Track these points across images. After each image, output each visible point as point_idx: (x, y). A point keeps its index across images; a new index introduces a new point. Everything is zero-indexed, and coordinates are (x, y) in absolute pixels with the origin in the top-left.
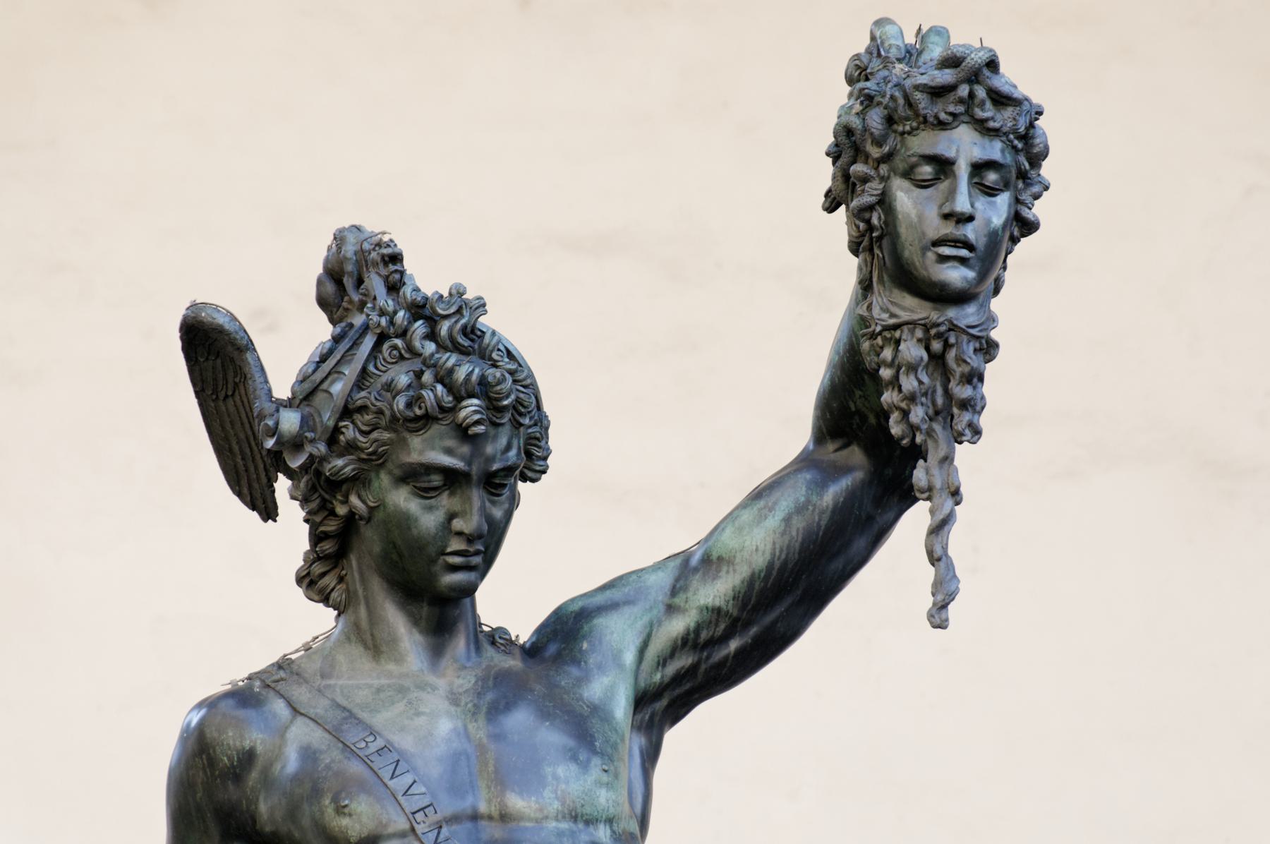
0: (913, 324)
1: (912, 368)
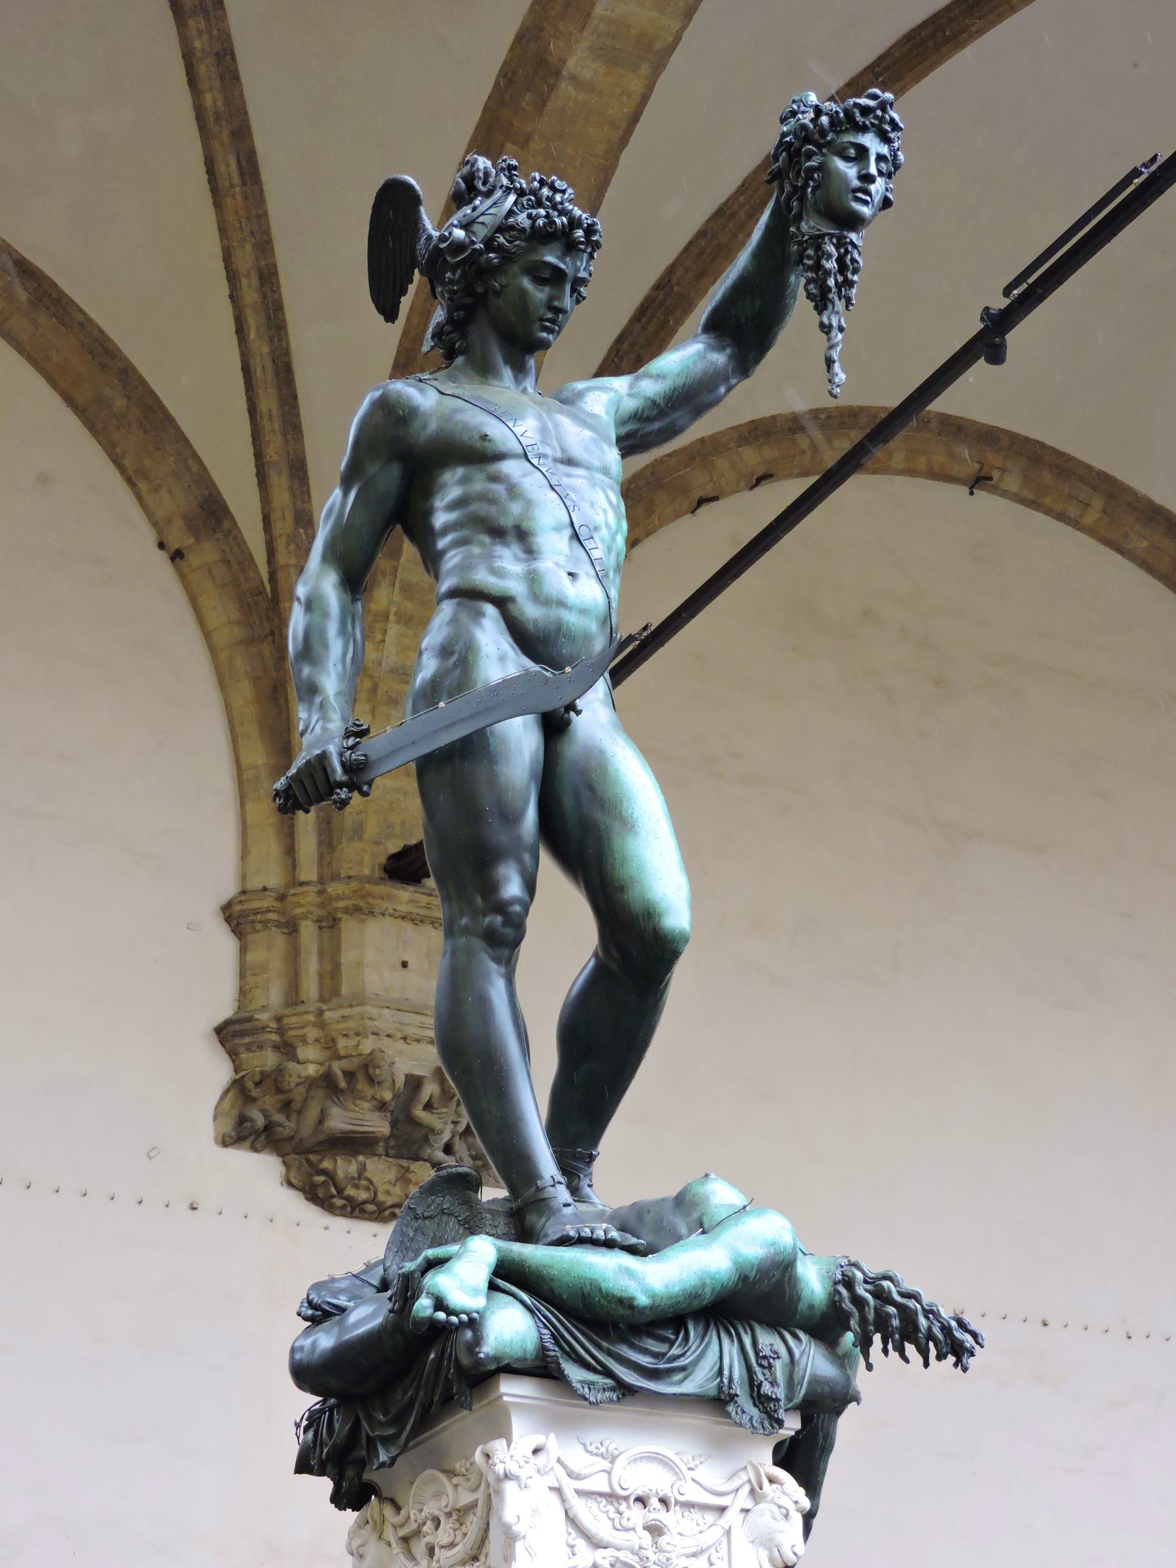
0: (831, 236)
1: (830, 256)
